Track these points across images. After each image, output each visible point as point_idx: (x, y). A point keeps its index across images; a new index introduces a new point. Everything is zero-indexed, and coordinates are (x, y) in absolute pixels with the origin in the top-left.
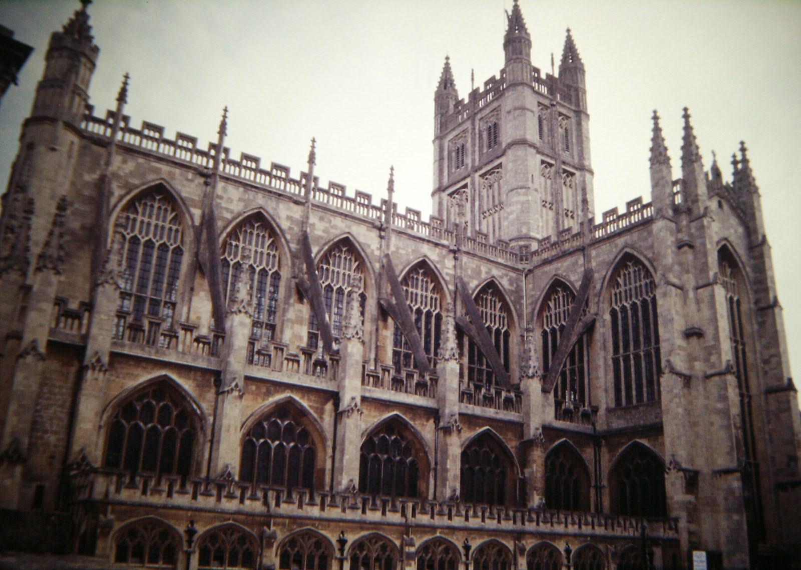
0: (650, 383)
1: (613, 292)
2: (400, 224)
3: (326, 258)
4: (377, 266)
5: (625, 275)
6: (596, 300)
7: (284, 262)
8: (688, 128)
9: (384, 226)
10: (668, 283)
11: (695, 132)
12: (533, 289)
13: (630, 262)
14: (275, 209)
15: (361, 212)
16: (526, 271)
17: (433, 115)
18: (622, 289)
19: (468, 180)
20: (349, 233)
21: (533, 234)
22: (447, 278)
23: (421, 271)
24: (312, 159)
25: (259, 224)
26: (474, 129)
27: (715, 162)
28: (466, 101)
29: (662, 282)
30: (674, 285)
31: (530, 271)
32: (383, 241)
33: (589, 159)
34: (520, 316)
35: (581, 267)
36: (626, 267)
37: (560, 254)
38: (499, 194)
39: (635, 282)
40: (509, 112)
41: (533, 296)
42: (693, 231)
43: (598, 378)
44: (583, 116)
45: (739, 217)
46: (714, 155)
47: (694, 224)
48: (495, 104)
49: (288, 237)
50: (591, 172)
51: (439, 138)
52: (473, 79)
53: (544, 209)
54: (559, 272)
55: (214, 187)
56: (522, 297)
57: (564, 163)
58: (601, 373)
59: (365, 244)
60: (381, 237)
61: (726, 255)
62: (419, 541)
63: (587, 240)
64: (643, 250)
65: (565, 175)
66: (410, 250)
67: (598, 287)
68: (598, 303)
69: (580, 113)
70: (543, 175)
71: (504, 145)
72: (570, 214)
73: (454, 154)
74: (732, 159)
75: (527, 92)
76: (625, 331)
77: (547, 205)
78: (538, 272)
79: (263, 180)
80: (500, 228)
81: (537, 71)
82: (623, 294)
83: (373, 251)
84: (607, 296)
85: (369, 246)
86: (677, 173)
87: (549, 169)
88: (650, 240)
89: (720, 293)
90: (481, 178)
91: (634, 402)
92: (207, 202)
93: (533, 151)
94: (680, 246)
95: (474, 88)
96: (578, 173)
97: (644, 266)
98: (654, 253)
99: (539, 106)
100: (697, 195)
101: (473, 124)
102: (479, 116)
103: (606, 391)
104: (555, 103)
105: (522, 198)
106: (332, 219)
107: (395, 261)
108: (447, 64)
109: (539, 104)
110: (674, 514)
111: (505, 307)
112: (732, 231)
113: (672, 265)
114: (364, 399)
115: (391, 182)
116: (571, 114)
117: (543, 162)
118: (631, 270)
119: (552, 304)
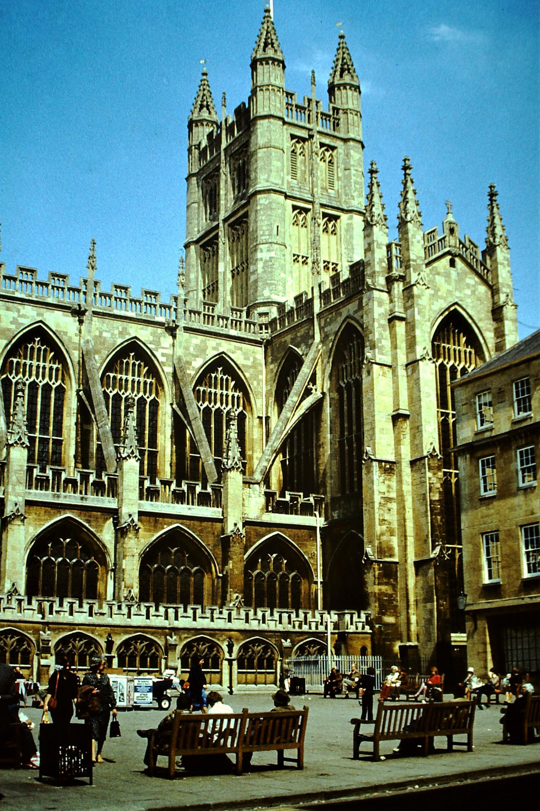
9: (83, 309)
20: (41, 321)
59: (61, 331)
60: (81, 322)
65: (326, 219)
66: (116, 332)
70: (295, 223)
77: (300, 259)
82: (349, 368)
83: (70, 338)
85: (65, 333)
87: (302, 216)
96: (344, 217)
99: (292, 139)
106: (20, 307)
109: (293, 137)
111: (241, 386)
114: (29, 503)
116: (338, 144)
117: (294, 208)
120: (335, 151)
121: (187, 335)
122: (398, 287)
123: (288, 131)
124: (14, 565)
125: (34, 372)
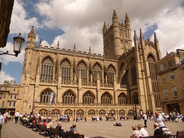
0: (136, 80)
2: (92, 57)
3: (78, 64)
4: (88, 65)
15: (84, 56)
21: (119, 55)
45: (154, 48)
48: (112, 31)
49: (71, 62)
53: (122, 50)
55: (58, 55)
60: (89, 59)
61: (150, 55)
62: (88, 110)
75: (117, 27)
79: (66, 53)
81: (119, 23)
83: (87, 62)
84: (130, 65)
89: (147, 63)
94: (140, 55)
96: (129, 42)
107: (91, 63)
109: (120, 29)
111: (114, 69)
115: (90, 49)
116: (127, 30)
121: (105, 61)
122: (141, 50)
123: (119, 29)
124: (80, 98)
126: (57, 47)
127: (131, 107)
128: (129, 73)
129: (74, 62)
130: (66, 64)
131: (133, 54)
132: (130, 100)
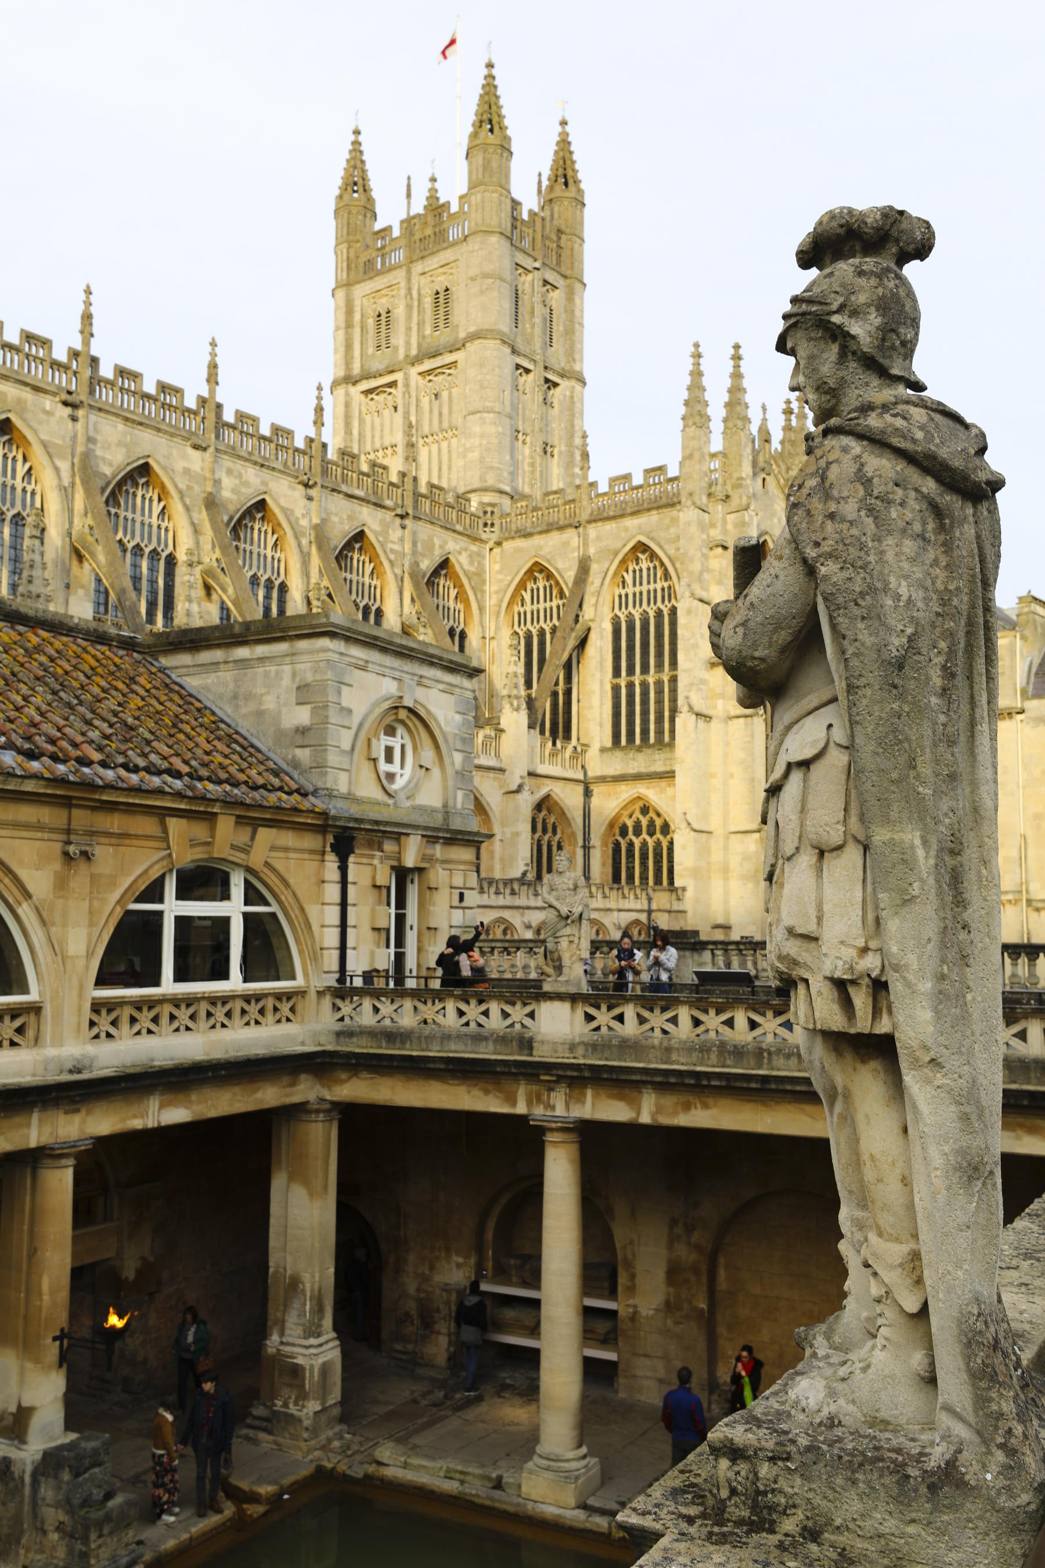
1: (617, 593)
4: (304, 542)
5: (634, 571)
6: (593, 600)
7: (179, 539)
8: (737, 375)
10: (693, 595)
11: (746, 383)
12: (500, 572)
13: (643, 552)
14: (167, 457)
16: (491, 544)
17: (332, 242)
18: (630, 590)
19: (398, 376)
22: (392, 557)
23: (357, 546)
24: (212, 378)
25: (143, 480)
26: (409, 290)
27: (765, 420)
28: (396, 232)
29: (687, 594)
30: (701, 601)
31: (499, 544)
32: (314, 505)
33: (582, 360)
34: (481, 609)
35: (573, 551)
36: (637, 560)
37: (544, 527)
38: (450, 412)
39: (649, 583)
40: (473, 279)
41: (501, 581)
42: (730, 527)
43: (591, 707)
44: (578, 286)
46: (764, 408)
47: (731, 518)
49: (188, 501)
50: (584, 383)
51: (345, 285)
52: (409, 195)
54: (542, 553)
56: (484, 582)
57: (546, 368)
58: (596, 701)
60: (310, 499)
63: (585, 516)
64: (662, 543)
67: (597, 582)
68: (596, 604)
69: (574, 279)
71: (462, 335)
72: (549, 450)
73: (371, 322)
74: (784, 406)
76: (631, 648)
78: (508, 545)
80: (450, 468)
81: (516, 204)
83: (297, 519)
84: (609, 598)
85: (292, 511)
86: (717, 444)
87: (525, 377)
88: (672, 530)
90: (420, 378)
91: (638, 741)
92: (80, 449)
93: (508, 350)
95: (412, 213)
96: (564, 384)
97: (662, 564)
98: (678, 549)
100: (742, 478)
101: (409, 279)
102: (418, 268)
103: (601, 725)
104: (537, 265)
105: (491, 429)
108: (356, 143)
110: (678, 883)
111: (461, 596)
112: (776, 521)
113: (701, 574)
116: (560, 282)
117: (518, 367)
118: (644, 565)
119: (527, 597)
120: (557, 292)
125: (255, 562)
126: (78, 346)
127: (639, 907)
128: (591, 649)
129: (211, 503)
130: (138, 518)
131: (654, 517)
132: (587, 848)
